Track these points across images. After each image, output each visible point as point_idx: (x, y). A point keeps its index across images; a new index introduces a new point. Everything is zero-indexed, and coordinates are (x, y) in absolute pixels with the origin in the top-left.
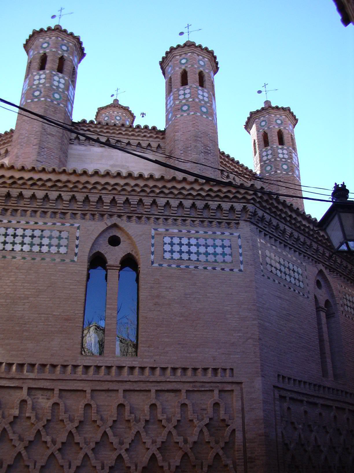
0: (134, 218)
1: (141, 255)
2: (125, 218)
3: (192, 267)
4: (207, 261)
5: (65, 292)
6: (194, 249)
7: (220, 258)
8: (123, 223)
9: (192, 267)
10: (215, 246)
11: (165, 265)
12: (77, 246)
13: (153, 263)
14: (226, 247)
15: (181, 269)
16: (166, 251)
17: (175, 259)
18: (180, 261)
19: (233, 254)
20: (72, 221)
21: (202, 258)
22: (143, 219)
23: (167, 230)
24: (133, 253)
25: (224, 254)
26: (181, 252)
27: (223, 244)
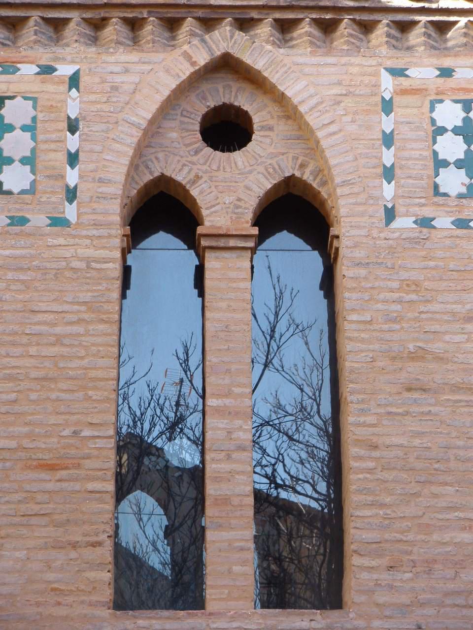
0: (306, 28)
1: (345, 183)
2: (265, 30)
5: (33, 351)
8: (259, 50)
11: (444, 222)
12: (73, 159)
13: (390, 214)
16: (445, 164)
20: (45, 56)
22: (345, 28)
24: (307, 176)
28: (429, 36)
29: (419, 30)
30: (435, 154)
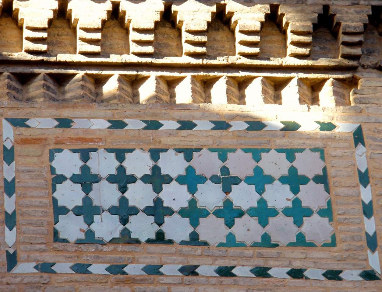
3: (171, 270)
4: (231, 241)
6: (175, 196)
7: (282, 228)
9: (171, 270)
10: (260, 180)
11: (63, 267)
13: (12, 260)
14: (304, 180)
15: (133, 281)
16: (64, 211)
17: (101, 242)
18: (120, 248)
19: (337, 209)
21: (212, 230)
23: (65, 123)
25: (298, 212)
26: (124, 211)
27: (293, 170)
28: (48, 88)
29: (38, 82)
30: (55, 201)
